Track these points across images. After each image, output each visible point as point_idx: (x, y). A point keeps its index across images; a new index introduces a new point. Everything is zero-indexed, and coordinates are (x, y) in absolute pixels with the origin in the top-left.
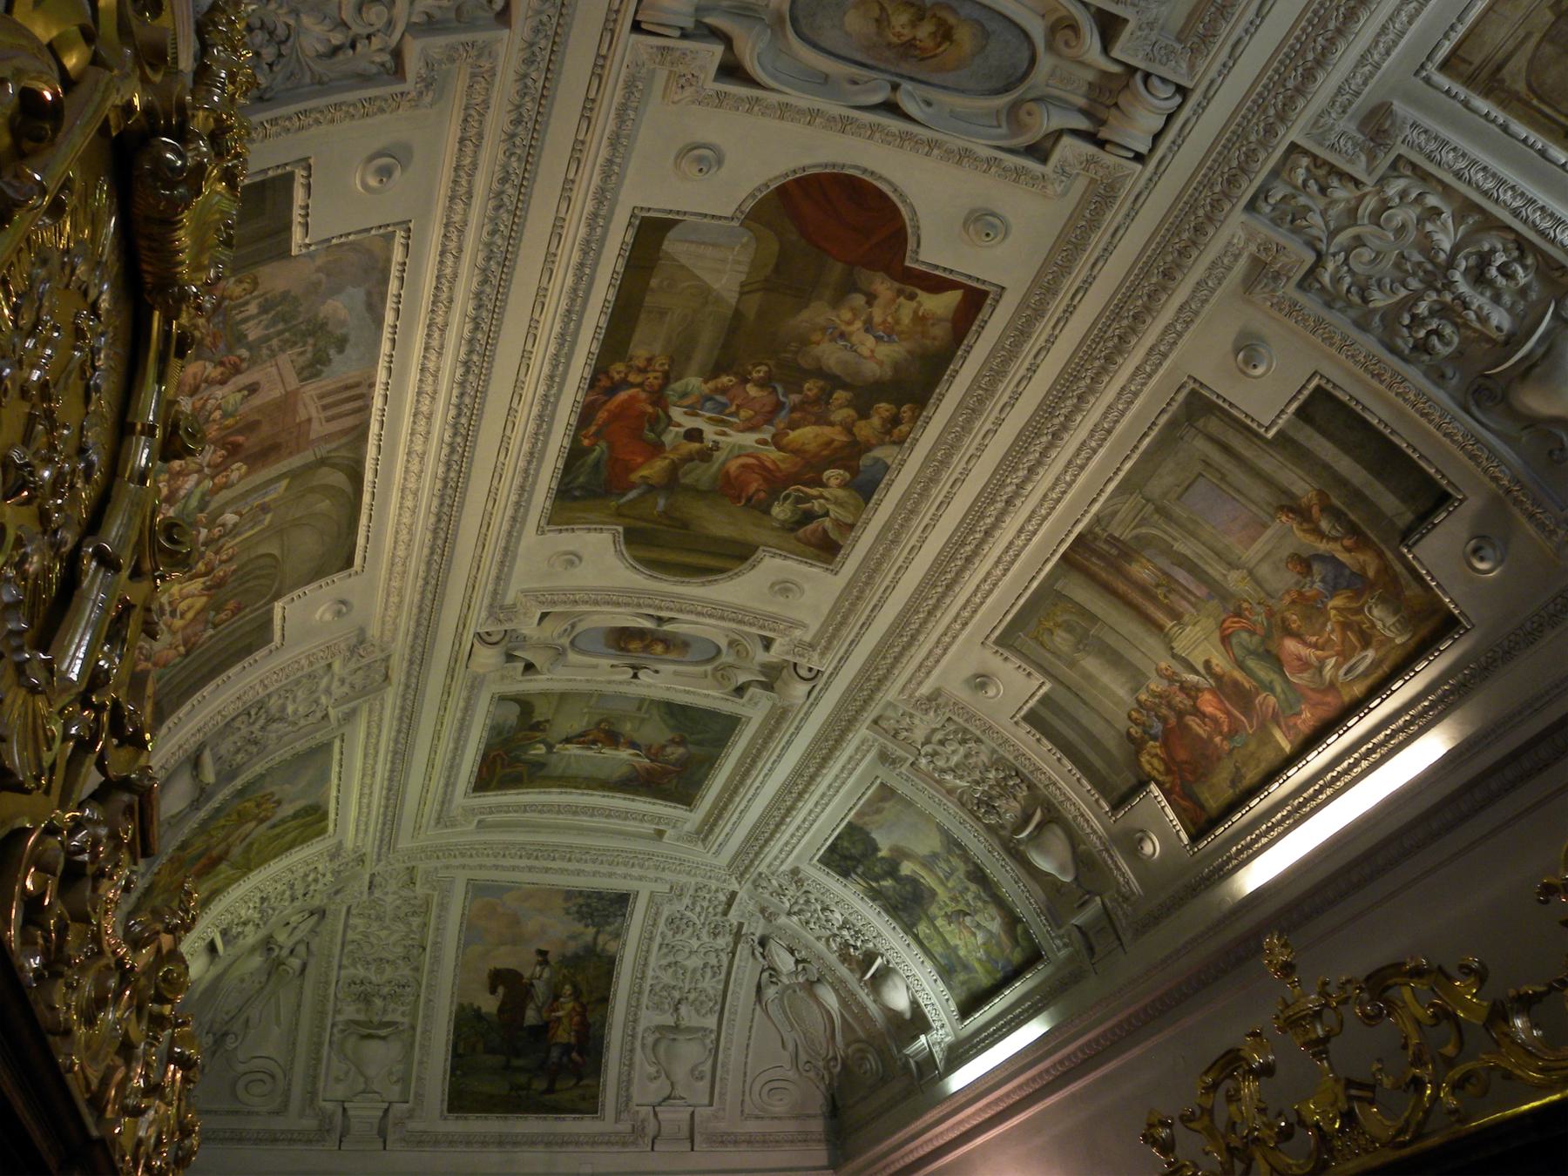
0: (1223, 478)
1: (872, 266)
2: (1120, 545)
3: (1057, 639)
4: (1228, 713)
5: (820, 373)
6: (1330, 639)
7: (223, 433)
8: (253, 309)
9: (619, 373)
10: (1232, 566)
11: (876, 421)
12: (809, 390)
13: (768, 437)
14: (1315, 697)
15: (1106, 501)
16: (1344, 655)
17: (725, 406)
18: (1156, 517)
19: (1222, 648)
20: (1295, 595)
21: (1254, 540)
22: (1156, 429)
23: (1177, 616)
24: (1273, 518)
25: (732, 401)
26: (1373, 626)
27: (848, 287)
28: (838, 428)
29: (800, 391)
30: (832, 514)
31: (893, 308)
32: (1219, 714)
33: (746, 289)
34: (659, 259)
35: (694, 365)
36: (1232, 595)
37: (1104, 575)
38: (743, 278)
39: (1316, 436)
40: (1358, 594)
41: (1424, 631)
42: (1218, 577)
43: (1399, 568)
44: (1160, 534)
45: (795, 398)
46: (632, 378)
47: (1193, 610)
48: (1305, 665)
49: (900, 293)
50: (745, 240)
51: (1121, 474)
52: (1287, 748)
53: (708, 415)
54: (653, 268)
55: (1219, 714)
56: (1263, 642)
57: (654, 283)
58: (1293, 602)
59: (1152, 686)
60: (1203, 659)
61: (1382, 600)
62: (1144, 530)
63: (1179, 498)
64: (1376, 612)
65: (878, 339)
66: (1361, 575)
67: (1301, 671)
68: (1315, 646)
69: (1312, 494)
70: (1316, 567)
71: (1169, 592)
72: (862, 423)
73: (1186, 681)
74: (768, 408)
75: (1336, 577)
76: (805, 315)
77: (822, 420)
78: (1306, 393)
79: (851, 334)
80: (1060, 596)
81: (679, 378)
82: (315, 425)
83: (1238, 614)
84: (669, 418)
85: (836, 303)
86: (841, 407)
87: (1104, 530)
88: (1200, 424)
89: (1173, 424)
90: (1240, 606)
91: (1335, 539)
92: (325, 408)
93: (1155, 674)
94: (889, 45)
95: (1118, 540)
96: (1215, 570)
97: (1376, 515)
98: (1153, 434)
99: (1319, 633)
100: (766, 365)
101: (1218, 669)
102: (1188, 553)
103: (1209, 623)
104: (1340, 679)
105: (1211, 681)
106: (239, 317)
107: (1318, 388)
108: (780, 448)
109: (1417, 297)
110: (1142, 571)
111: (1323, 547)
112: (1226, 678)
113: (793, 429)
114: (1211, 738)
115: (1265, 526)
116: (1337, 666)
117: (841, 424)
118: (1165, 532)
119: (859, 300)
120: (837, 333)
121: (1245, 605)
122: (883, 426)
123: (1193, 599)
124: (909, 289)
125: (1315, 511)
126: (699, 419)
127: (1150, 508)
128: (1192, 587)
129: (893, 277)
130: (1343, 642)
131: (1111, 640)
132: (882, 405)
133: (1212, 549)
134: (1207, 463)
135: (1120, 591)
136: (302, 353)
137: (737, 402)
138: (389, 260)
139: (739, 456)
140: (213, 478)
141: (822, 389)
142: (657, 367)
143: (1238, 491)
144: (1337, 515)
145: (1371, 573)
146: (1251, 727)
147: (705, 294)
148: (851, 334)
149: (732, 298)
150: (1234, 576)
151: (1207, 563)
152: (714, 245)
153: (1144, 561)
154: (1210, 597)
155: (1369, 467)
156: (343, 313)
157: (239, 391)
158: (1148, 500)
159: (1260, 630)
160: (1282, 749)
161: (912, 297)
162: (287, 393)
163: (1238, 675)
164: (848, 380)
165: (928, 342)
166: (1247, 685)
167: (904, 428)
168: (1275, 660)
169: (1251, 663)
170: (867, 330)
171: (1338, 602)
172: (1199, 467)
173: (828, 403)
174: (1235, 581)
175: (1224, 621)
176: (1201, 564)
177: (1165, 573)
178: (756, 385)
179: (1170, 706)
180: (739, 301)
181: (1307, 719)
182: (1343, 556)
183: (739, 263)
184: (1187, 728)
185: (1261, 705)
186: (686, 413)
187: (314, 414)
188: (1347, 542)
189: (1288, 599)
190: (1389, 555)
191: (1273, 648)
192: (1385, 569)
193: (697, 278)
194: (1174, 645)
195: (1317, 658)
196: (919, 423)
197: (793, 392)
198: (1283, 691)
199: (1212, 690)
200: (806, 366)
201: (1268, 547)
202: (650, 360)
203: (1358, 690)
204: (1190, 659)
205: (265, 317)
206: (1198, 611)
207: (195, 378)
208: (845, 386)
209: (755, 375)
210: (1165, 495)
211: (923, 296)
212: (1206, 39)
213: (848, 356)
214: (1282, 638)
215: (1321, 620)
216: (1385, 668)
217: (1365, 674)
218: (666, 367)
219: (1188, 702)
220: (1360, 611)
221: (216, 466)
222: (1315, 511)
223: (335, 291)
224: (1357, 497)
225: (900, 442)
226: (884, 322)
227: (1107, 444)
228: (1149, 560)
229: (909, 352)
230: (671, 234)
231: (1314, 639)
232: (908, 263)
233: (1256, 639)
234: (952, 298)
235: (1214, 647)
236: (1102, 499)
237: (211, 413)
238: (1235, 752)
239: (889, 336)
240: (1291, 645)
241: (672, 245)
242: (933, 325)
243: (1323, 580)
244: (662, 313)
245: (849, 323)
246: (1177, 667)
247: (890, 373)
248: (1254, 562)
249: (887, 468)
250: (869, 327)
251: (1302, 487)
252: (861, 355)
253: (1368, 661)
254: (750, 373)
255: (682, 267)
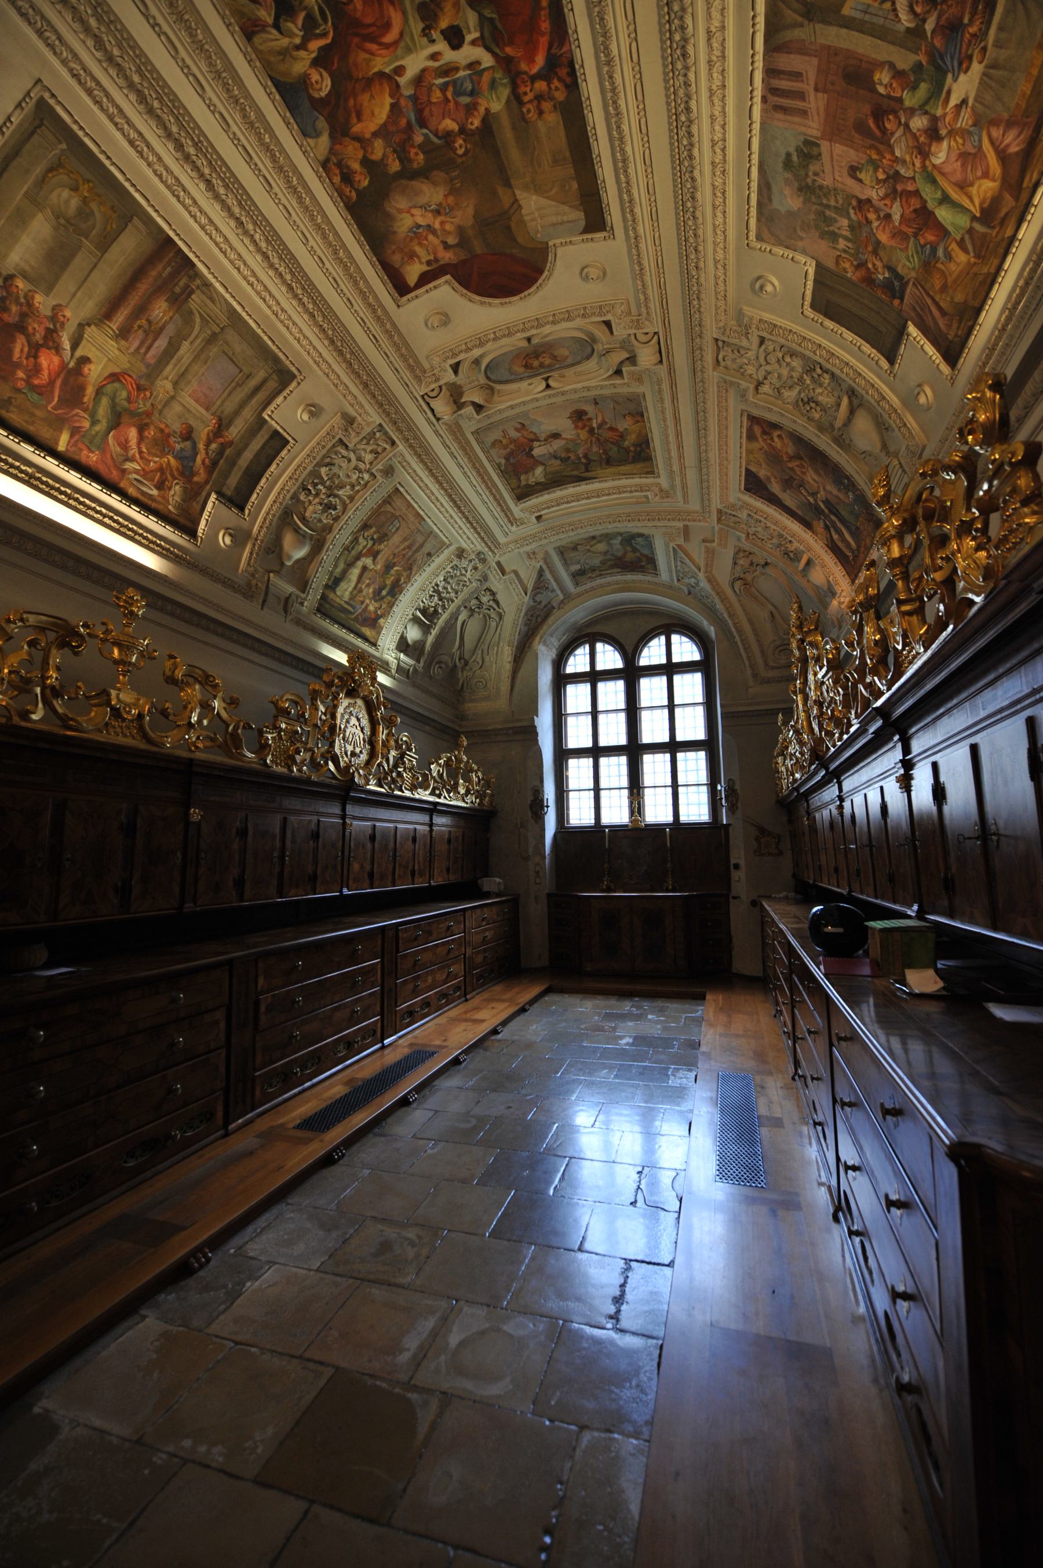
0: (239, 385)
1: (464, 262)
2: (184, 296)
3: (66, 193)
4: (51, 383)
5: (423, 174)
6: (149, 461)
7: (881, 147)
8: (842, 244)
9: (557, 89)
10: (175, 384)
11: (356, 166)
12: (417, 154)
13: (402, 81)
14: (109, 461)
15: (225, 300)
16: (145, 474)
17: (457, 93)
18: (209, 332)
19: (106, 374)
20: (167, 431)
21: (197, 401)
22: (277, 351)
23: (124, 333)
24: (213, 414)
25: (456, 103)
26: (170, 489)
27: (463, 242)
28: (368, 136)
29: (420, 146)
30: (274, 32)
31: (431, 250)
32: (46, 373)
33: (515, 206)
34: (581, 204)
35: (505, 121)
36: (153, 384)
37: (154, 273)
38: (524, 212)
39: (263, 441)
40: (182, 474)
41: (182, 520)
42: (165, 373)
43: (204, 494)
44: (195, 332)
45: (419, 139)
46: (541, 85)
47: (132, 350)
48: (125, 446)
49: (436, 260)
50: (539, 235)
51: (247, 318)
52: (62, 447)
53: (461, 73)
54: (582, 196)
55: (46, 373)
56: (126, 410)
57: (575, 185)
58: (162, 431)
59: (38, 298)
60: (90, 356)
61: (185, 490)
62: (198, 320)
63: (224, 352)
64: (177, 487)
65: (419, 226)
66: (193, 474)
67: (119, 445)
68: (141, 452)
69: (230, 438)
70: (188, 444)
71: (145, 331)
72: (360, 155)
73: (60, 337)
74: (426, 113)
75: (186, 458)
76: (470, 211)
77: (382, 132)
78: (287, 436)
79: (435, 217)
80: (125, 221)
81: (508, 102)
82: (811, 75)
83: (140, 388)
84: (488, 49)
85: (461, 231)
86: (384, 155)
87: (198, 287)
88: (274, 376)
89: (276, 360)
90: (145, 389)
91: (207, 453)
92: (801, 96)
93: (54, 303)
94: (544, 352)
95: (189, 295)
96: (170, 371)
97: (226, 475)
98: (274, 348)
99: (149, 453)
100: (461, 156)
101: (86, 370)
102: (181, 352)
103: (123, 363)
104: (130, 476)
105: (72, 365)
106: (850, 245)
107: (288, 442)
108: (381, 74)
109: (323, 483)
110: (160, 310)
111: (201, 446)
112: (81, 378)
113: (393, 105)
114: (18, 365)
115: (207, 409)
116: (136, 472)
117: (369, 140)
118: (197, 337)
119: (451, 240)
120: (442, 211)
121: (148, 394)
122: (348, 167)
123: (142, 351)
124: (435, 266)
125: (221, 440)
126: (464, 62)
127: (217, 330)
128: (152, 352)
129: (447, 265)
130: (152, 471)
131: (81, 261)
132: (366, 183)
133: (186, 370)
134: (249, 376)
135: (139, 285)
136: (816, 174)
137: (452, 105)
138: (758, 220)
139: (401, 34)
140: (900, 100)
141: (410, 161)
142: (530, 106)
143: (230, 394)
144: (221, 452)
145: (196, 479)
146: (54, 408)
147: (539, 190)
148: (435, 217)
149: (520, 194)
150: (169, 386)
151: (175, 365)
152: (553, 225)
153: (171, 314)
154: (148, 366)
155: (248, 468)
156: (787, 191)
157: (861, 181)
158: (222, 329)
159: (132, 407)
160: (57, 444)
161: (429, 263)
162: (830, 140)
163: (90, 391)
164: (404, 182)
165: (394, 247)
166: (85, 399)
167: (337, 179)
168: (116, 422)
169: (105, 401)
170: (429, 226)
171: (173, 461)
172: (246, 370)
173: (395, 151)
174: (164, 386)
175: (130, 376)
176: (173, 361)
177: (162, 329)
178: (452, 131)
179: (23, 316)
180: (514, 193)
181: (92, 458)
182: (199, 459)
183: (532, 220)
184: (13, 340)
185: (77, 415)
186: (478, 63)
187: (812, 93)
188: (207, 461)
189: (162, 426)
190: (208, 487)
191: (125, 419)
192: (201, 487)
193: (548, 198)
194: (93, 327)
195: (134, 455)
196: (336, 194)
197: (423, 142)
198: (97, 433)
199: (63, 365)
200: (435, 173)
201: (194, 411)
202: (541, 113)
203: (131, 491)
204: (84, 342)
205: (836, 230)
206: (133, 354)
207: (884, 228)
208: (400, 175)
209: (461, 141)
210: (226, 343)
211: (425, 268)
212: (452, 432)
213: (422, 200)
214: (134, 426)
215: (158, 453)
216: (154, 505)
217: (143, 493)
218: (524, 110)
219: (38, 337)
220: (174, 478)
221: (895, 112)
222: (221, 440)
223: (790, 214)
224: (232, 463)
225: (325, 164)
226: (426, 239)
227: (273, 317)
228: (171, 318)
229: (395, 233)
230: (583, 223)
231: (145, 450)
232: (448, 277)
233: (125, 404)
234: (412, 279)
235: (105, 367)
236: (227, 296)
237: (885, 181)
238: (23, 396)
239: (415, 233)
240: (133, 433)
241: (578, 216)
242: (403, 259)
243: (182, 449)
244: (556, 162)
245: (442, 223)
246: (71, 328)
247: (388, 209)
248: (181, 400)
249: (305, 134)
250: (429, 228)
251: (234, 432)
252: (415, 207)
253: (151, 492)
254: (464, 140)
255: (563, 203)
